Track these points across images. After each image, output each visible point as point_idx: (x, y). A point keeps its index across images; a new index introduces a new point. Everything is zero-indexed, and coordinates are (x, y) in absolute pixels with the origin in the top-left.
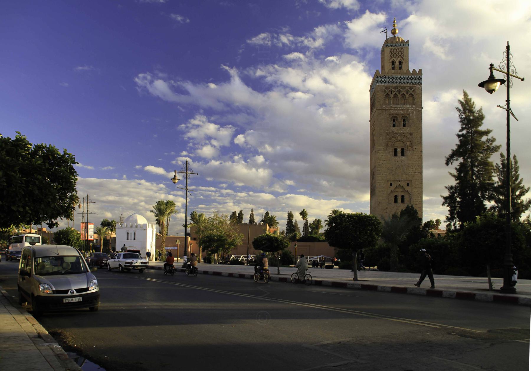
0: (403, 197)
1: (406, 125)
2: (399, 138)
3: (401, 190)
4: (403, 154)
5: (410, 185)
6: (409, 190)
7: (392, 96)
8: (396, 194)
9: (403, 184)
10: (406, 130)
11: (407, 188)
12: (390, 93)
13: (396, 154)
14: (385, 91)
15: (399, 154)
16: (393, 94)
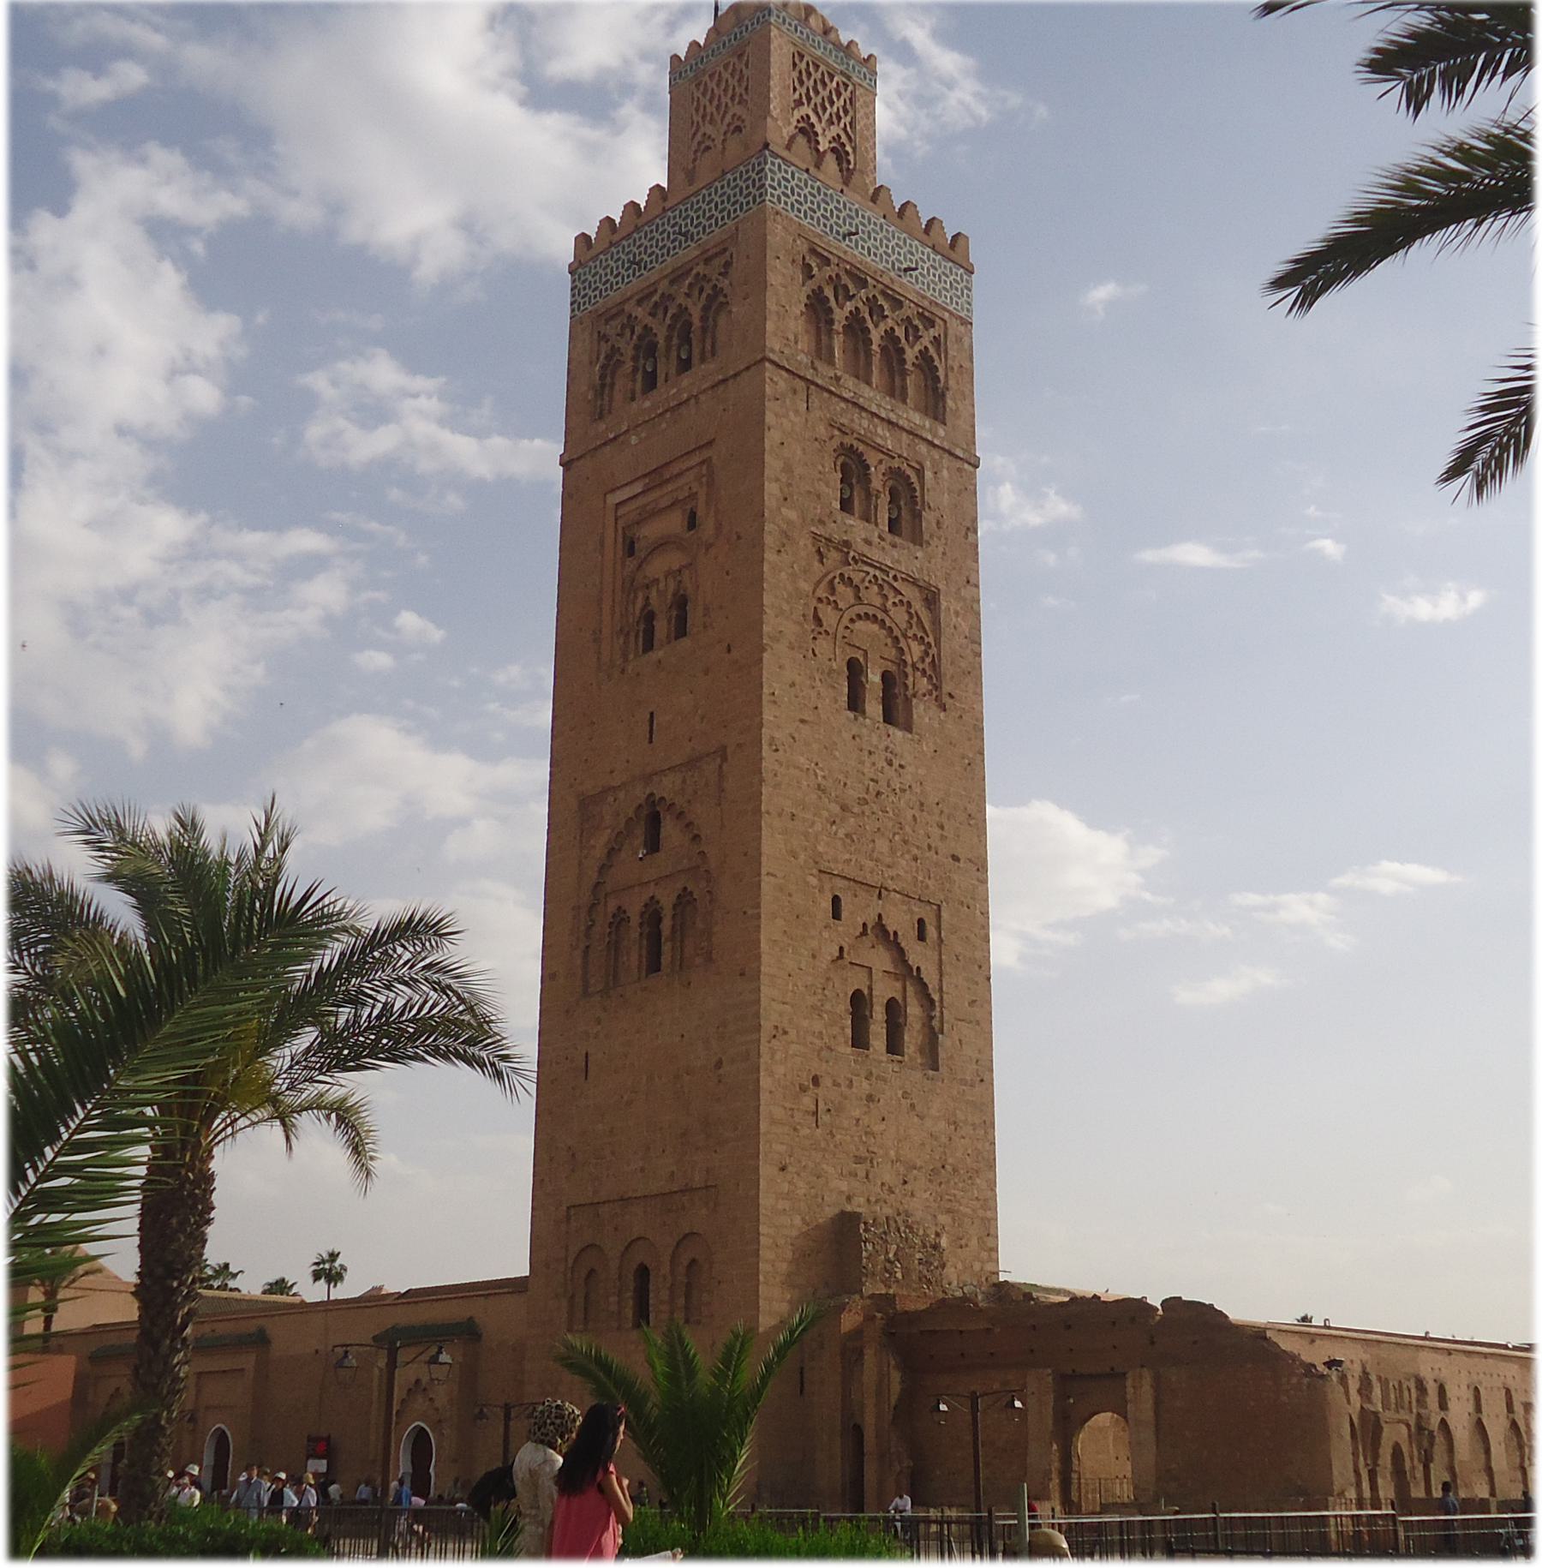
0: (892, 1007)
1: (905, 524)
2: (872, 595)
3: (880, 960)
4: (888, 718)
5: (931, 931)
6: (930, 976)
7: (840, 316)
8: (858, 981)
9: (899, 920)
10: (900, 557)
11: (918, 956)
12: (829, 292)
13: (855, 703)
14: (807, 268)
15: (874, 708)
16: (849, 306)
